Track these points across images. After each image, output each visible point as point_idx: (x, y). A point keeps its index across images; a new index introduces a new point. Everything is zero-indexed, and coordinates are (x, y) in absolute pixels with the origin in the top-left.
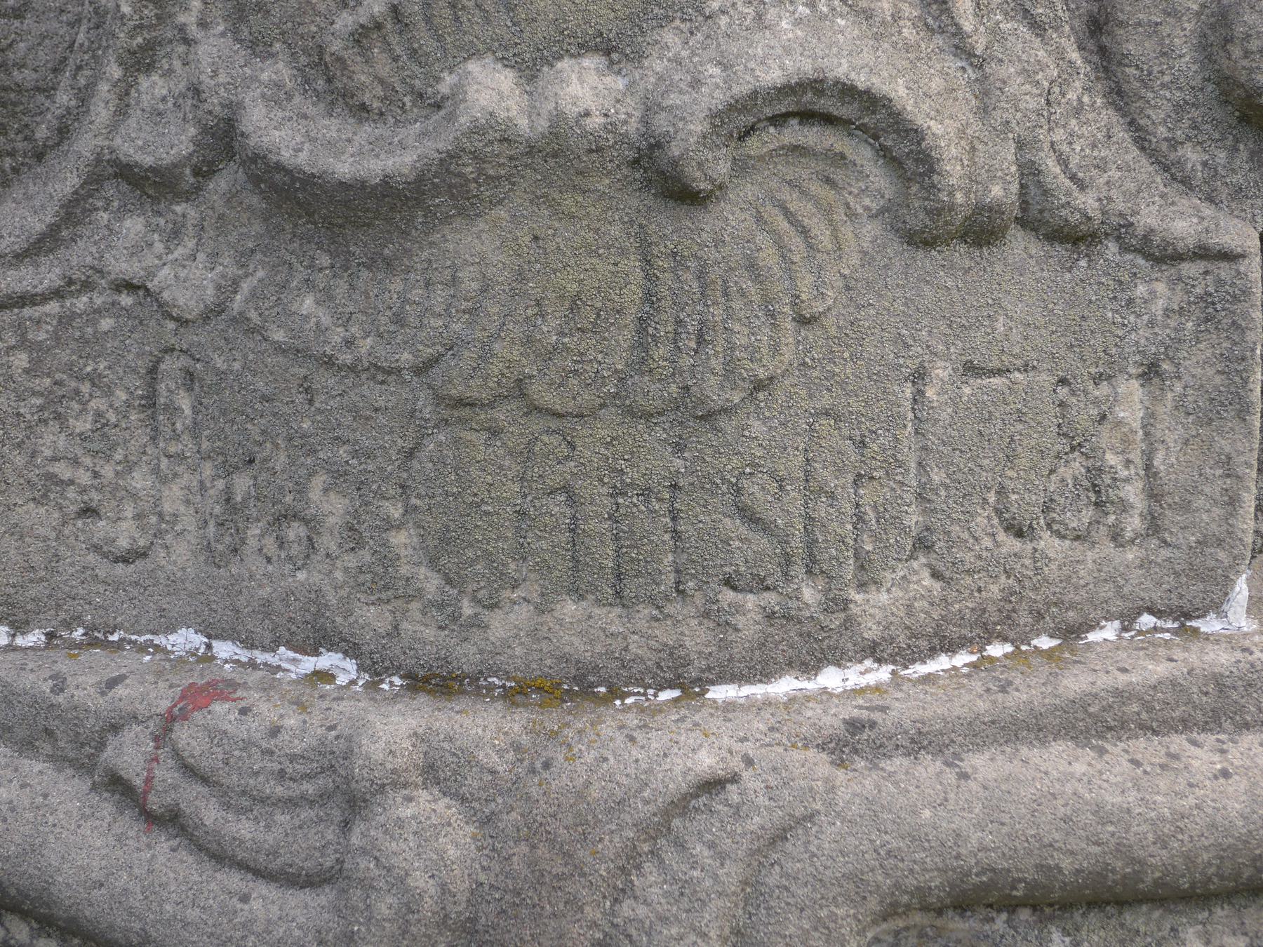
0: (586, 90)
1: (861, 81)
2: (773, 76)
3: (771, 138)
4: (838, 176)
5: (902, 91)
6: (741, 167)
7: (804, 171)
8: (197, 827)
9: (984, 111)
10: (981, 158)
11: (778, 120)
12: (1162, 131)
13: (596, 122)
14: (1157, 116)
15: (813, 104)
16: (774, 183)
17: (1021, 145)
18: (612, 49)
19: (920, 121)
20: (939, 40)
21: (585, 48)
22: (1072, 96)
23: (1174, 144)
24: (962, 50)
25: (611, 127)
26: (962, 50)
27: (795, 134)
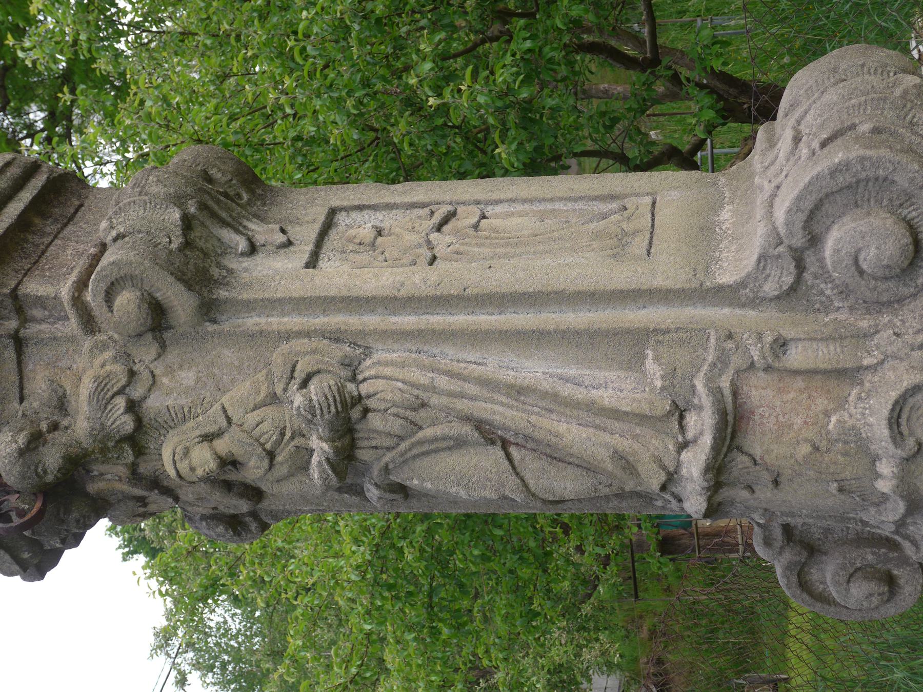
0: (886, 468)
1: (890, 407)
2: (886, 432)
3: (904, 429)
4: (917, 406)
5: (894, 394)
6: (911, 434)
7: (914, 416)
8: (215, 601)
9: (902, 359)
10: (915, 364)
11: (899, 425)
12: (912, 290)
13: (895, 470)
14: (906, 291)
15: (895, 420)
16: (917, 424)
17: (912, 350)
18: (875, 459)
19: (903, 390)
20: (878, 368)
21: (874, 465)
22: (899, 323)
23: (917, 286)
24: (882, 362)
25: (898, 467)
26: (882, 362)
27: (903, 421)
